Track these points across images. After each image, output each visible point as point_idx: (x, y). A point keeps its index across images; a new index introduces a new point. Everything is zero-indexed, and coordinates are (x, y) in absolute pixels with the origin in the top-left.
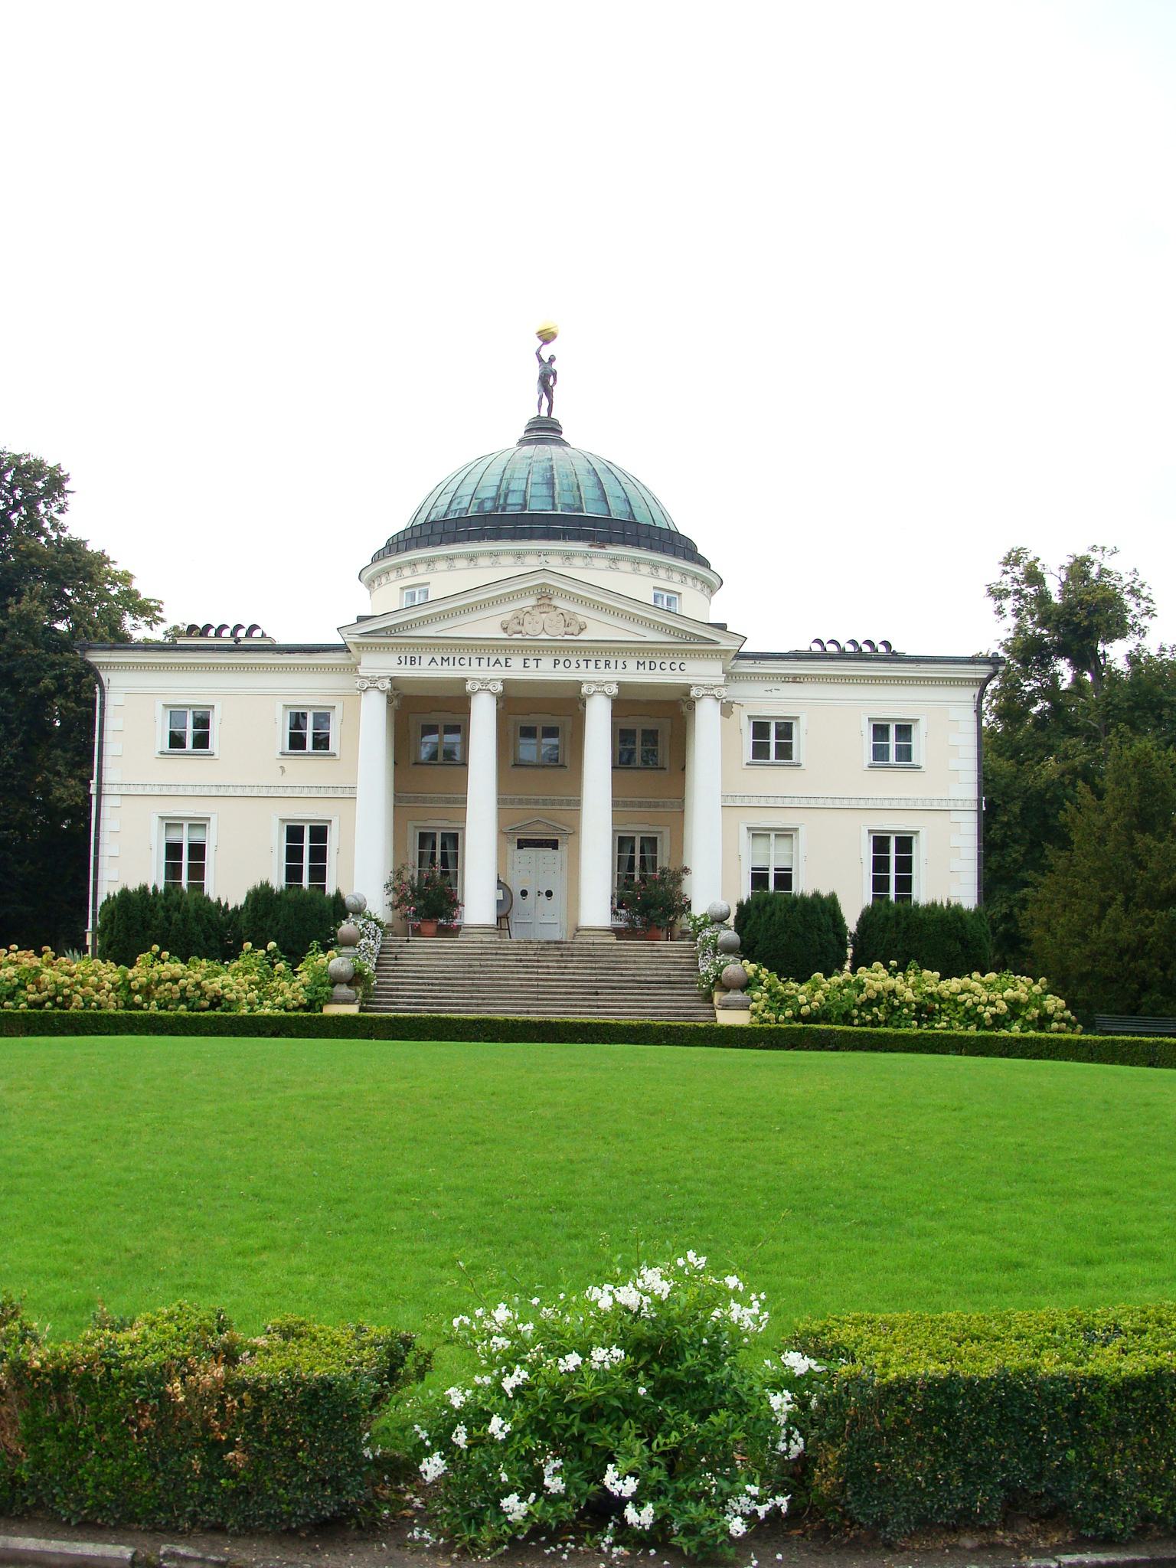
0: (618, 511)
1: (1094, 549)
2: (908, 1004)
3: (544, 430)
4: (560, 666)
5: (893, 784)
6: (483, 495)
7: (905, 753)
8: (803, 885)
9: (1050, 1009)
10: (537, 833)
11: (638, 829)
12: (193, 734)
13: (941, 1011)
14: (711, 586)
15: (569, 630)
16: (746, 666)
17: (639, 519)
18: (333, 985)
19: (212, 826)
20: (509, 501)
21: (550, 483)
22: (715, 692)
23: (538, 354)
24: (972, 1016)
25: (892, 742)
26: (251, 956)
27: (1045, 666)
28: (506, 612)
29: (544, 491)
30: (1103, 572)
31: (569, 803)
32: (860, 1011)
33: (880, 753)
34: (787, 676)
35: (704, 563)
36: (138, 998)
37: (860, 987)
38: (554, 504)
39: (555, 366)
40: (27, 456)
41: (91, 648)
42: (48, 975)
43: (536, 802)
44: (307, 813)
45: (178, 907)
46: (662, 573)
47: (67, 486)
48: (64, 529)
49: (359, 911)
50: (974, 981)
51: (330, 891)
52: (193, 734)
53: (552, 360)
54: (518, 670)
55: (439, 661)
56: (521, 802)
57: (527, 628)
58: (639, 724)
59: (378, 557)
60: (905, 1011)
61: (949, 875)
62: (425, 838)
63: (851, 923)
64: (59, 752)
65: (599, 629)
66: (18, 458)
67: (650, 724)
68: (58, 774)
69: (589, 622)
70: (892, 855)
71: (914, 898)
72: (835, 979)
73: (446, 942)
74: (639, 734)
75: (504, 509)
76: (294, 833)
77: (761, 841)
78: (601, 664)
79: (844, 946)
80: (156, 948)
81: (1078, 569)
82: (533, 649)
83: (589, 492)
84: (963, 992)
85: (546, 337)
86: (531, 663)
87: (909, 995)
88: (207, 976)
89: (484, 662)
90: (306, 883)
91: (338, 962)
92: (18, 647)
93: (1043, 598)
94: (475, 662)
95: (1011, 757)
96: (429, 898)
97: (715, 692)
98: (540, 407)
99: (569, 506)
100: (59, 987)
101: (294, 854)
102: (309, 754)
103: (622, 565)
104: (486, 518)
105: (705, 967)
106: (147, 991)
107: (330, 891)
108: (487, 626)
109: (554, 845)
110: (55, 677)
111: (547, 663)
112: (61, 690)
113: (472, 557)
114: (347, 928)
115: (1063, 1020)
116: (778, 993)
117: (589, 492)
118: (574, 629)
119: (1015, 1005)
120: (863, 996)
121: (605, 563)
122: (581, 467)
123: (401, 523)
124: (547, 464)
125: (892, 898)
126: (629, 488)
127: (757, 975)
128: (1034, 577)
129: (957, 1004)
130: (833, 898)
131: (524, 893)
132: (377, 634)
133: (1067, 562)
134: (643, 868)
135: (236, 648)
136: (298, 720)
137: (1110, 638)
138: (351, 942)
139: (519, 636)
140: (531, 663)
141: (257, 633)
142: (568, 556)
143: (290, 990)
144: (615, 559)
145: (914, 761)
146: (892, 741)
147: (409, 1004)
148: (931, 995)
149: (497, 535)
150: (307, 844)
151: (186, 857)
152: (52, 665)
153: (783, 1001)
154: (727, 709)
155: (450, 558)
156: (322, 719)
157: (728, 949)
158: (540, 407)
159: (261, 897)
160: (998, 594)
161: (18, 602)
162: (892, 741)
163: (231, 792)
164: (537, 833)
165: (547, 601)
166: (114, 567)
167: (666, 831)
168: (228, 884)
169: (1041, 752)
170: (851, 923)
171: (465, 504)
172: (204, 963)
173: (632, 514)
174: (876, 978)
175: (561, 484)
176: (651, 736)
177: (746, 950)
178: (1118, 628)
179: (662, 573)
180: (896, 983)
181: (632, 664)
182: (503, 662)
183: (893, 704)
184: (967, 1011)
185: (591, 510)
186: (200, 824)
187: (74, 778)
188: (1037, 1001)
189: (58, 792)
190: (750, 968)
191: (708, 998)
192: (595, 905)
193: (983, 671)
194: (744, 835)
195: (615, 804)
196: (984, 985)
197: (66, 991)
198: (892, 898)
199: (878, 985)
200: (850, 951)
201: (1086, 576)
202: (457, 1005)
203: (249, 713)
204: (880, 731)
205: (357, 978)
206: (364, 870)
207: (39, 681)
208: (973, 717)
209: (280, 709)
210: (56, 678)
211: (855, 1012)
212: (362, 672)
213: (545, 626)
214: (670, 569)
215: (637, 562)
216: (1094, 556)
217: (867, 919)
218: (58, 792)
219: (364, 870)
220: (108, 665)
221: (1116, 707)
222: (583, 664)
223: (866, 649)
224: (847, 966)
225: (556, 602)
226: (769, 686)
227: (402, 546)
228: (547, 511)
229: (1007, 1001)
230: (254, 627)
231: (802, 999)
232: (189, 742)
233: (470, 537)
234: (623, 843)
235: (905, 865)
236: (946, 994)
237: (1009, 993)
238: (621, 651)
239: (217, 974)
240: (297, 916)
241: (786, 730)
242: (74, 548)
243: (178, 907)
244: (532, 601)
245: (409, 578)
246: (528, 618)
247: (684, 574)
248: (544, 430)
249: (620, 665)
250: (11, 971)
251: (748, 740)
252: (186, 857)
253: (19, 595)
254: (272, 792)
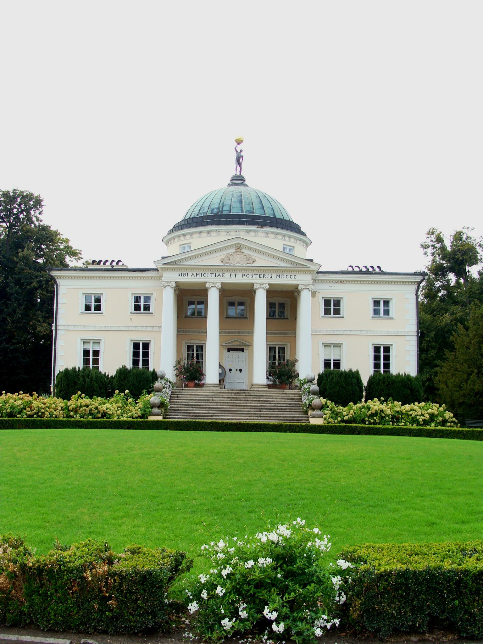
0: (268, 213)
1: (464, 228)
2: (388, 416)
3: (238, 180)
4: (245, 277)
5: (382, 324)
6: (213, 207)
7: (387, 312)
8: (344, 367)
9: (447, 417)
10: (236, 347)
11: (277, 343)
13: (402, 418)
14: (307, 244)
15: (249, 262)
16: (321, 277)
17: (277, 216)
18: (152, 408)
19: (102, 342)
20: (224, 209)
21: (241, 202)
22: (308, 287)
23: (235, 149)
24: (414, 420)
25: (382, 308)
26: (118, 396)
27: (444, 276)
28: (222, 255)
29: (238, 205)
30: (468, 238)
31: (249, 333)
32: (369, 418)
33: (376, 312)
34: (338, 281)
35: (304, 234)
36: (72, 413)
37: (369, 408)
38: (242, 210)
39: (242, 154)
40: (26, 191)
41: (52, 270)
42: (35, 404)
43: (235, 333)
44: (141, 338)
45: (88, 376)
46: (287, 238)
47: (43, 203)
48: (41, 221)
49: (162, 378)
50: (416, 406)
51: (151, 369)
52: (95, 305)
53: (241, 151)
54: (228, 279)
55: (195, 275)
56: (229, 332)
57: (231, 261)
58: (277, 300)
59: (170, 232)
60: (387, 418)
61: (405, 362)
62: (190, 348)
63: (365, 382)
64: (39, 312)
65: (261, 261)
66: (23, 192)
67: (282, 301)
68: (39, 321)
69: (257, 259)
70: (382, 354)
71: (391, 372)
72: (359, 405)
73: (198, 390)
74: (277, 305)
75: (222, 212)
76: (136, 346)
77: (327, 348)
78: (262, 276)
79: (362, 392)
80: (79, 393)
81: (458, 237)
82: (234, 270)
83: (257, 205)
84: (411, 410)
85: (239, 142)
86: (233, 276)
87: (389, 412)
88: (100, 404)
89: (214, 275)
90: (141, 366)
91: (154, 398)
92: (23, 269)
93: (443, 248)
94: (210, 275)
95: (431, 314)
96: (192, 373)
97: (308, 287)
98: (236, 170)
99: (249, 211)
100: (39, 409)
101: (136, 354)
102: (142, 313)
103: (270, 235)
104: (215, 216)
105: (305, 400)
106: (75, 410)
107: (151, 369)
108: (215, 260)
109: (242, 350)
110: (38, 282)
111: (239, 275)
112: (40, 287)
113: (209, 232)
114: (157, 384)
115: (452, 422)
116: (335, 411)
117: (257, 205)
118: (251, 261)
119: (432, 416)
120: (370, 412)
121: (263, 234)
122: (253, 195)
123: (179, 219)
124: (239, 194)
125: (382, 372)
126: (273, 204)
127: (326, 403)
128: (439, 239)
129: (408, 415)
130: (357, 372)
131: (230, 370)
132: (171, 264)
133: (453, 233)
134: (279, 359)
135: (112, 270)
136: (137, 299)
137: (471, 264)
138: (159, 390)
139: (228, 264)
140: (233, 276)
141: (120, 264)
142: (248, 231)
143: (135, 409)
144: (267, 233)
145: (391, 315)
146: (381, 307)
147: (183, 416)
148: (398, 412)
149: (219, 223)
150: (141, 350)
151: (91, 355)
152: (37, 277)
153: (337, 414)
154: (313, 294)
155: (200, 233)
156: (147, 299)
157: (314, 393)
158: (236, 170)
159: (122, 372)
160: (425, 247)
161: (23, 251)
162: (381, 307)
163: (110, 329)
164: (236, 347)
165: (239, 250)
166: (62, 237)
167: (289, 344)
168: (109, 367)
169: (443, 311)
170: (365, 382)
171: (206, 210)
172: (99, 399)
173: (274, 214)
174: (375, 405)
175: (245, 202)
176: (282, 305)
177: (322, 393)
178: (474, 261)
179: (287, 238)
180: (384, 407)
181: (274, 276)
182: (221, 275)
183: (382, 292)
184: (413, 418)
185: (257, 213)
186: (97, 342)
187: (46, 323)
188: (441, 414)
189: (39, 329)
190: (323, 400)
191: (306, 413)
192: (260, 374)
193: (419, 278)
194: (321, 346)
195: (267, 333)
196: (420, 408)
197: (43, 411)
198: (382, 372)
199: (376, 408)
200: (364, 394)
201: (461, 239)
202: (203, 416)
203: (117, 295)
204: (376, 303)
205: (161, 405)
206: (164, 361)
207: (31, 283)
208: (415, 297)
209: (130, 295)
210: (38, 282)
211: (367, 419)
212: (163, 279)
213: (238, 261)
214: (290, 237)
215: (276, 234)
216: (464, 231)
217: (371, 380)
218: (39, 329)
219: (164, 361)
220: (60, 277)
221: (474, 293)
222: (254, 276)
223: (371, 269)
224: (363, 400)
225: (243, 250)
226: (331, 285)
227: (180, 228)
229: (429, 414)
230: (119, 261)
231: (345, 413)
232: (93, 308)
233: (208, 224)
234: (271, 349)
235: (387, 358)
236: (404, 411)
237: (430, 411)
238: (270, 270)
239: (105, 403)
240: (137, 380)
241: (338, 303)
242: (45, 229)
243: (88, 376)
244: (232, 250)
245: (183, 241)
246: (231, 257)
247: (296, 239)
248: (238, 180)
249: (270, 276)
250: (20, 402)
251: (322, 307)
252: (91, 355)
253: (23, 248)
254: (127, 329)
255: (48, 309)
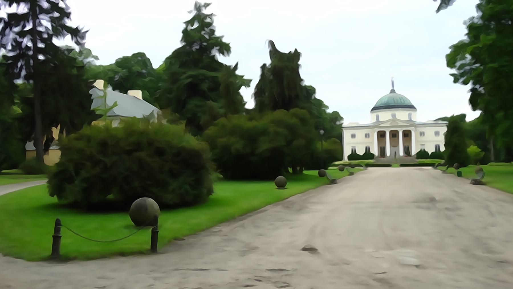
11: (406, 145)
12: (353, 136)
44: (367, 145)
52: (353, 136)
59: (372, 110)
108: (387, 124)
117: (399, 100)
150: (368, 149)
192: (401, 153)
219: (375, 151)
228: (394, 104)
255: (340, 138)
